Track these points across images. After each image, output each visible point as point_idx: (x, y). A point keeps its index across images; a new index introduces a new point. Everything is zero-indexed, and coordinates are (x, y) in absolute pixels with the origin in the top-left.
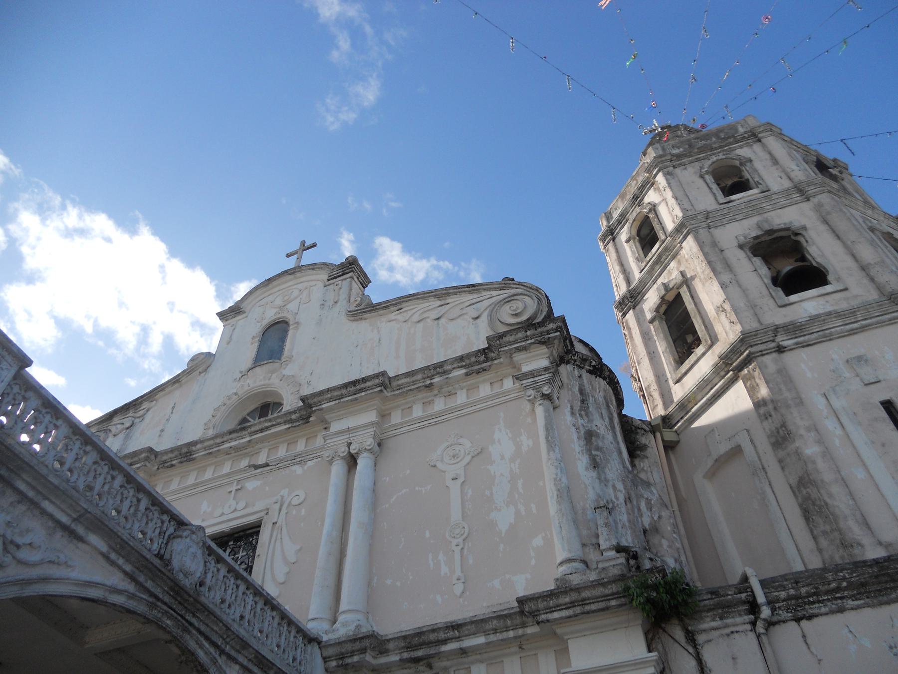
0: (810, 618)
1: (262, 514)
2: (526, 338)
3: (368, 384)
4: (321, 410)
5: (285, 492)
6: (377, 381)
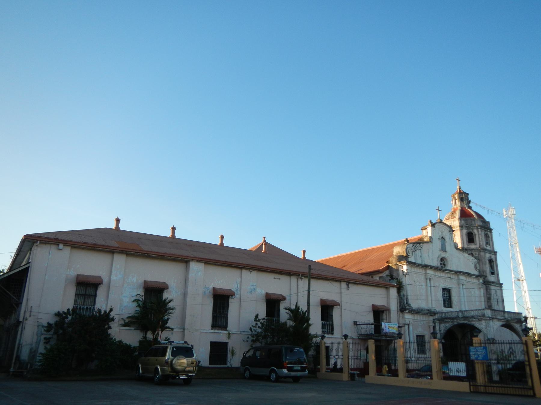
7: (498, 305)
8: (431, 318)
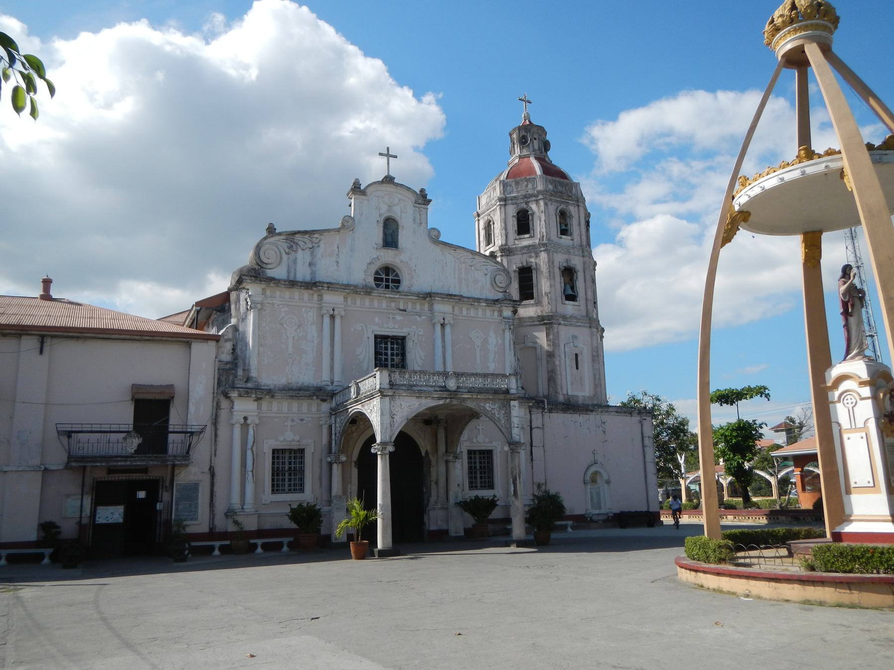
1: (407, 334)
3: (455, 298)
4: (435, 300)
5: (414, 327)
6: (459, 298)
7: (577, 368)
8: (325, 407)
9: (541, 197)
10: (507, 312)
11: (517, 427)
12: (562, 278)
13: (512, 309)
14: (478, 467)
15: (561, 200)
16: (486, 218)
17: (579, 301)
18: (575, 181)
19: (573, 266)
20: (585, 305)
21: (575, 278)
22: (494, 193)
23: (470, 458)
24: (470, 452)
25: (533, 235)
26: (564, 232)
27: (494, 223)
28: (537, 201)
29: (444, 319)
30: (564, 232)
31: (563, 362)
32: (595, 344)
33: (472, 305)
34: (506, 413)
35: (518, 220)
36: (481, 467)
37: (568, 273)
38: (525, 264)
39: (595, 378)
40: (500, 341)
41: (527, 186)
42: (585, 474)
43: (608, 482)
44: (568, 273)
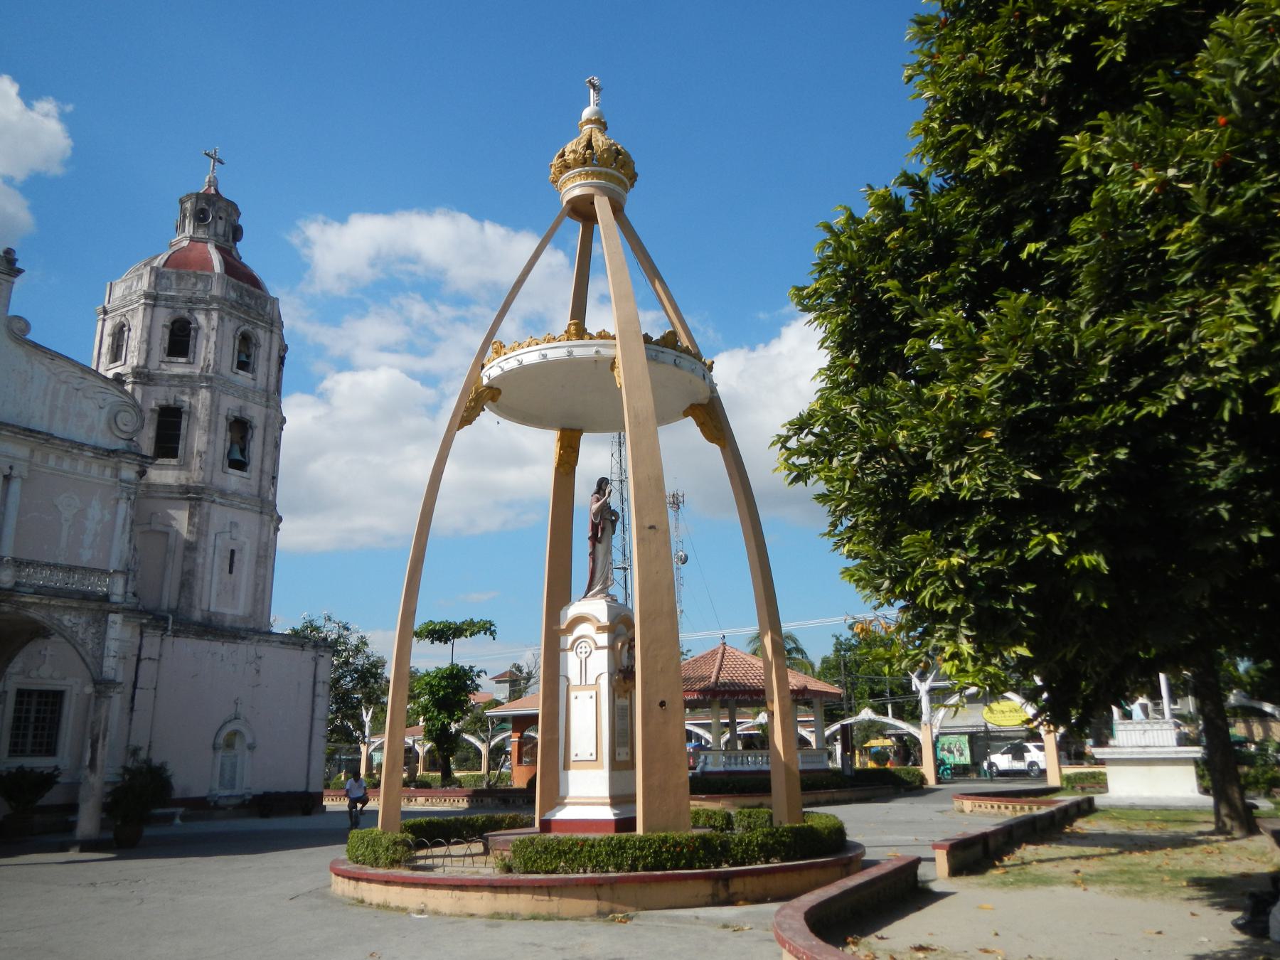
0: (178, 637)
2: (134, 460)
3: (40, 436)
6: (45, 437)
7: (231, 572)
9: (215, 306)
10: (129, 472)
11: (115, 657)
12: (229, 433)
13: (137, 468)
14: (32, 719)
15: (246, 318)
16: (118, 320)
17: (250, 472)
18: (272, 294)
19: (248, 418)
20: (258, 479)
21: (249, 437)
22: (137, 285)
23: (19, 703)
24: (21, 693)
25: (192, 361)
26: (243, 365)
27: (130, 330)
28: (208, 312)
29: (11, 468)
30: (243, 365)
31: (209, 560)
32: (264, 539)
33: (67, 451)
34: (97, 632)
35: (173, 334)
36: (37, 719)
37: (240, 428)
38: (171, 402)
39: (256, 590)
40: (108, 517)
41: (195, 284)
42: (217, 734)
43: (251, 747)
44: (240, 428)
